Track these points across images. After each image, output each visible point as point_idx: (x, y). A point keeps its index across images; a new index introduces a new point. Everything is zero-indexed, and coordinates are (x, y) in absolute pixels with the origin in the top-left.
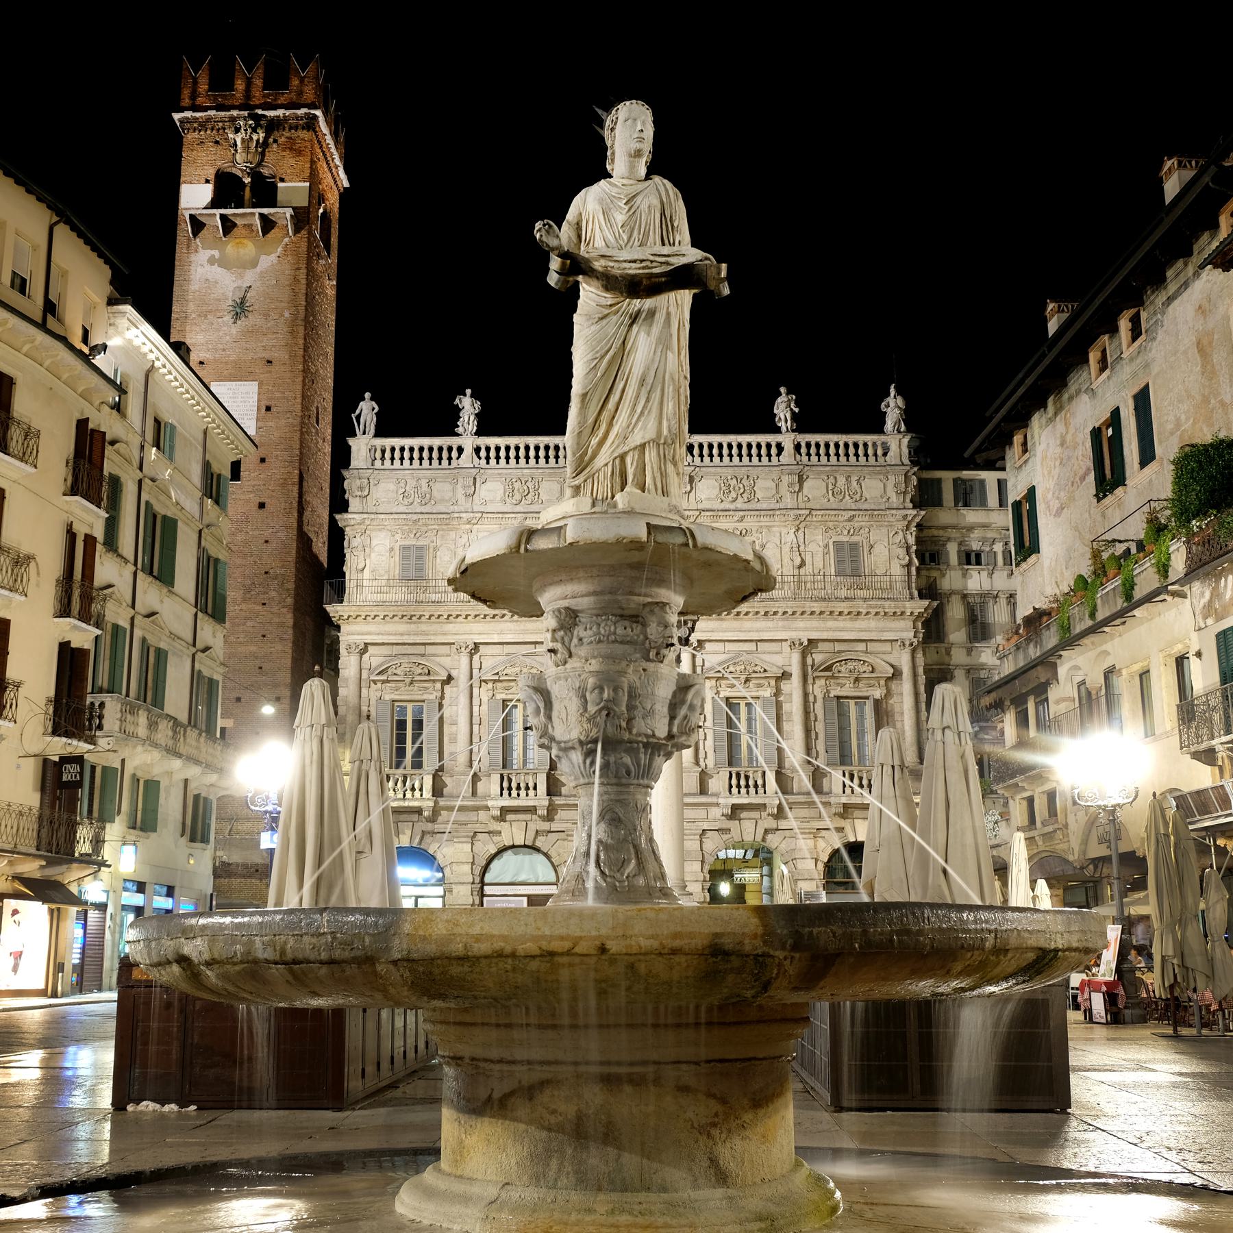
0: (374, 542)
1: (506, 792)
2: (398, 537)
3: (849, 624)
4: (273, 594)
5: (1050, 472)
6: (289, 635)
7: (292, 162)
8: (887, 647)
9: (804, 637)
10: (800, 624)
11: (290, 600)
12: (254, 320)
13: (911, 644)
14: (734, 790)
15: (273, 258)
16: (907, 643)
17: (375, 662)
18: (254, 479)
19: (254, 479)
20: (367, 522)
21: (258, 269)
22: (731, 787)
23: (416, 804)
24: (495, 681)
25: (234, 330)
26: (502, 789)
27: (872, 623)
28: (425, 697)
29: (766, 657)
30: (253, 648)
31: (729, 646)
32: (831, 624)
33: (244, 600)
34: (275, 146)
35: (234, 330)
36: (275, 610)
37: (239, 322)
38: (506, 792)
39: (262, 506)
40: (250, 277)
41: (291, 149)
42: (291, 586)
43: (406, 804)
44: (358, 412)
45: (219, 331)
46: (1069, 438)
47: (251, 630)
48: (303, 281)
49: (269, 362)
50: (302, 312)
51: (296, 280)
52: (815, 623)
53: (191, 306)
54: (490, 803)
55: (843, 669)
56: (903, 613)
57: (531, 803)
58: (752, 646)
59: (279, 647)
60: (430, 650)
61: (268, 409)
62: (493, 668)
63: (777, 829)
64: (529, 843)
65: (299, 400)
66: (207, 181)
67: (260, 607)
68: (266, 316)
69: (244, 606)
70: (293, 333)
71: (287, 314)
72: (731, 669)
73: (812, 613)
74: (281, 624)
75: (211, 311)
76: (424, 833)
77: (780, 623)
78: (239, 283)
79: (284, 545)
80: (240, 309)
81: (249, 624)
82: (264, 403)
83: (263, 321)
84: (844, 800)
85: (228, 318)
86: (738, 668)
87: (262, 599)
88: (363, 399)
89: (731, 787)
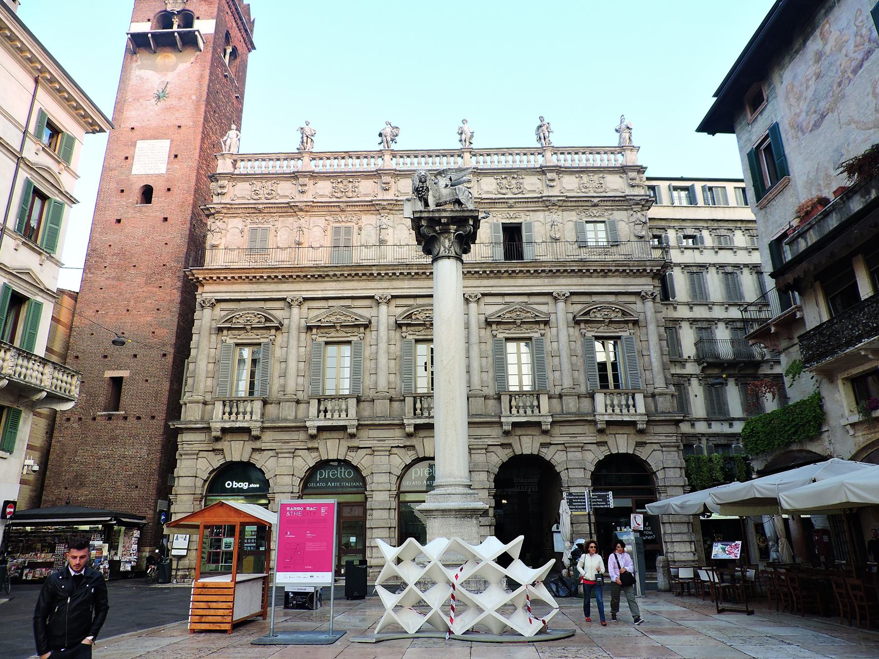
0: (230, 226)
1: (322, 414)
2: (249, 221)
3: (601, 281)
5: (798, 99)
7: (206, 8)
8: (632, 299)
9: (567, 290)
10: (562, 281)
11: (179, 284)
13: (652, 294)
14: (514, 411)
15: (188, 64)
16: (650, 293)
17: (223, 313)
18: (161, 202)
19: (161, 202)
20: (225, 211)
21: (177, 71)
22: (511, 407)
23: (245, 425)
24: (318, 327)
25: (156, 108)
26: (319, 411)
27: (620, 280)
28: (262, 340)
29: (535, 306)
30: (149, 319)
31: (508, 299)
32: (586, 280)
33: (146, 284)
39: (166, 219)
40: (170, 77)
43: (238, 425)
44: (225, 138)
46: (828, 49)
47: (149, 305)
49: (179, 127)
50: (204, 97)
51: (202, 76)
52: (575, 281)
53: (129, 94)
54: (308, 424)
55: (599, 316)
56: (645, 270)
57: (342, 423)
58: (525, 299)
60: (269, 305)
61: (176, 156)
62: (317, 316)
63: (551, 444)
64: (341, 457)
65: (198, 151)
66: (149, 20)
67: (157, 289)
68: (179, 99)
69: (145, 289)
70: (197, 108)
71: (194, 97)
72: (508, 315)
73: (573, 271)
76: (254, 450)
77: (546, 280)
78: (163, 79)
79: (179, 246)
84: (607, 418)
85: (153, 101)
86: (514, 315)
87: (158, 284)
88: (230, 129)
89: (511, 407)
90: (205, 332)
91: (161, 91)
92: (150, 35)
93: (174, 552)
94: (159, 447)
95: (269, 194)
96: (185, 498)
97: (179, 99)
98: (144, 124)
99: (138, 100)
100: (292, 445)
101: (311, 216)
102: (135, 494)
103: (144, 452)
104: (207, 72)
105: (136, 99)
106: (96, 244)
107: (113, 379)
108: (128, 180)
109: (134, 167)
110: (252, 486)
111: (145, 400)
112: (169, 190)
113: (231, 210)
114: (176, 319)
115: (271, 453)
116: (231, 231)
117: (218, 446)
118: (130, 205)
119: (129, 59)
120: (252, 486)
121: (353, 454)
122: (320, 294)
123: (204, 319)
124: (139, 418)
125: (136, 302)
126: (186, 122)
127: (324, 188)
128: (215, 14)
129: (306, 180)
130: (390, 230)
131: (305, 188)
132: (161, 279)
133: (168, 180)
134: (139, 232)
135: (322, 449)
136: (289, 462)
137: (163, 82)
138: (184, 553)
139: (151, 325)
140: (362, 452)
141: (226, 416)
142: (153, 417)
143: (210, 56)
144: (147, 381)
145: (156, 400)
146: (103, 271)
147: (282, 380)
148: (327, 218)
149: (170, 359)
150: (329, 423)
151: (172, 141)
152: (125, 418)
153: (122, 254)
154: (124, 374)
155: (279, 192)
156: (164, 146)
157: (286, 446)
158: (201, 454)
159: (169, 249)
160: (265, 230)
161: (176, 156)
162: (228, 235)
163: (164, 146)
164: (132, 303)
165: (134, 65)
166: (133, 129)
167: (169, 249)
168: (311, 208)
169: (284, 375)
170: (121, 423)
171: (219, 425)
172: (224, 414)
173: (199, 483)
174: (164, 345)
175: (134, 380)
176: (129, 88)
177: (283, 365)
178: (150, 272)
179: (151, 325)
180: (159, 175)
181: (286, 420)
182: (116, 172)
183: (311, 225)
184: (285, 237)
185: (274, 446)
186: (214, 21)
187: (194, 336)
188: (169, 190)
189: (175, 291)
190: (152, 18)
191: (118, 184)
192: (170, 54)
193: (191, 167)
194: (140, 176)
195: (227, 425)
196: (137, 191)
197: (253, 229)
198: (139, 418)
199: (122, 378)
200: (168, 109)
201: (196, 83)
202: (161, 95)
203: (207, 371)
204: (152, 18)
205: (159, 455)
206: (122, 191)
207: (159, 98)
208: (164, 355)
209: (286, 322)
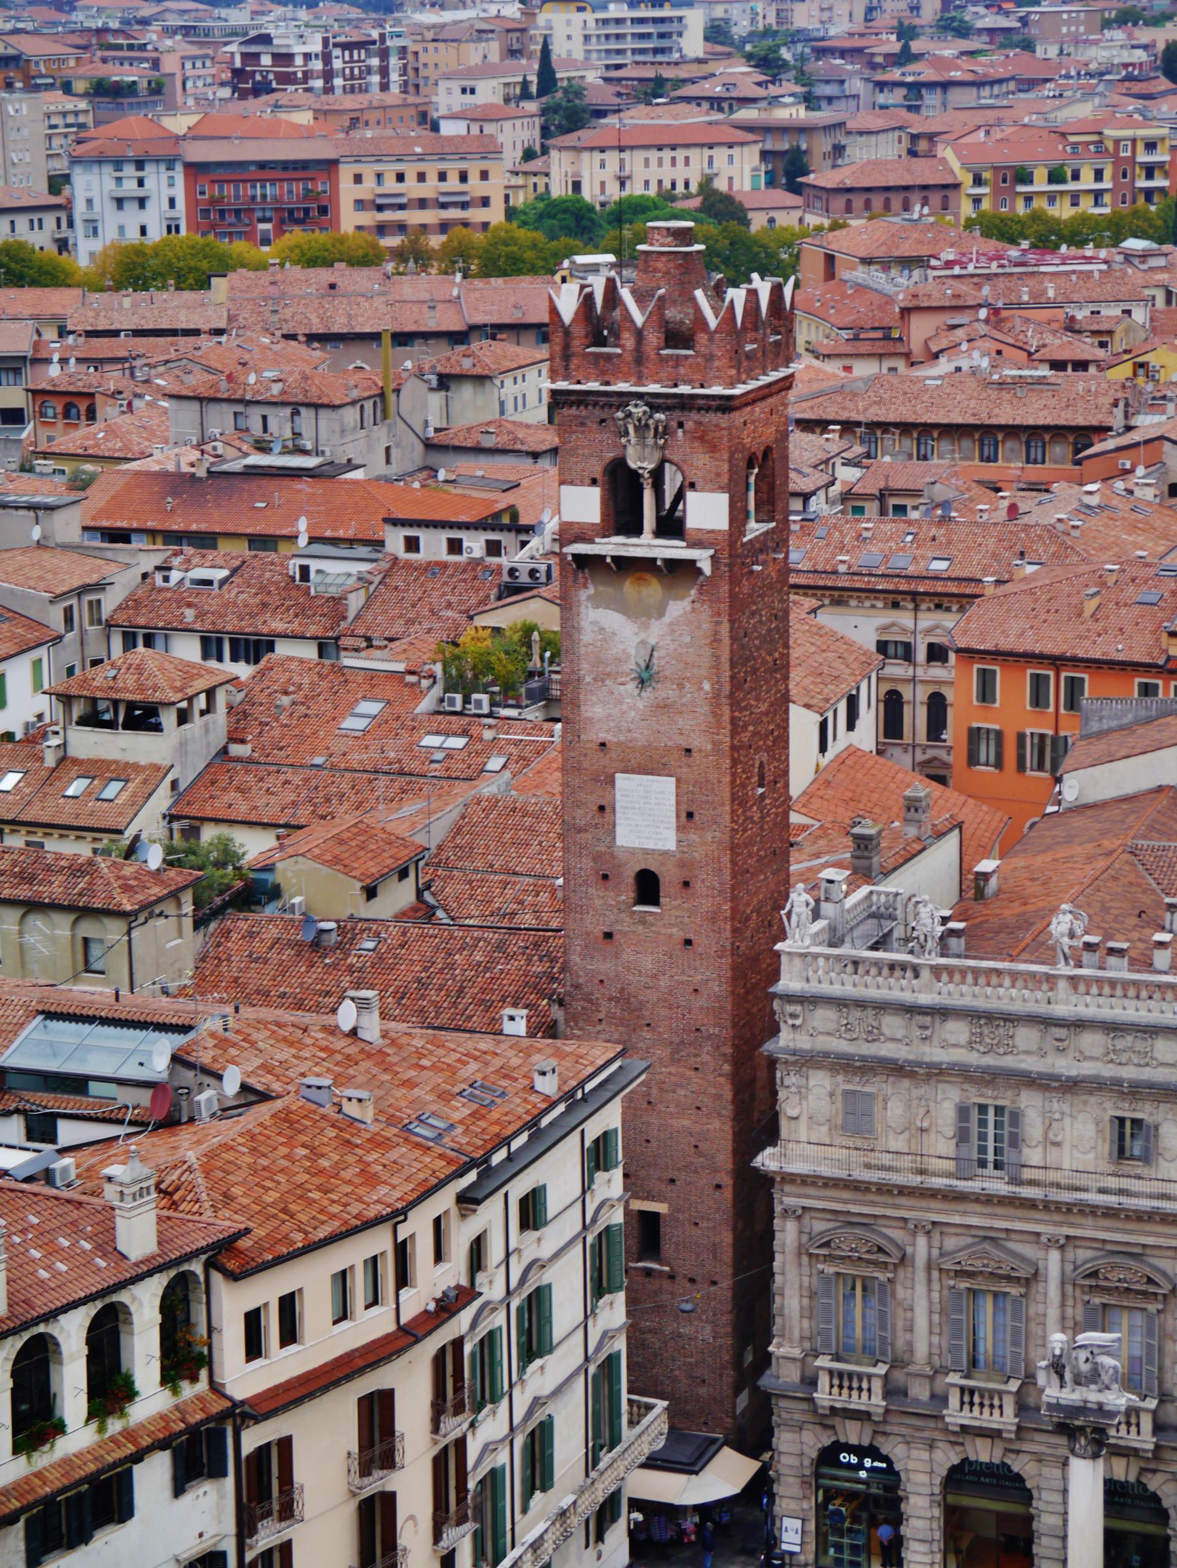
0: (812, 1083)
1: (966, 1407)
4: (706, 1058)
6: (728, 1111)
11: (727, 1068)
12: (666, 691)
18: (676, 908)
19: (676, 908)
21: (667, 619)
26: (962, 1403)
30: (686, 1122)
34: (680, 432)
35: (640, 704)
36: (711, 1077)
37: (643, 694)
38: (966, 1407)
39: (688, 942)
40: (656, 631)
41: (702, 439)
42: (729, 1050)
43: (852, 1406)
45: (621, 703)
48: (727, 641)
49: (688, 751)
50: (726, 689)
51: (715, 640)
53: (585, 665)
59: (717, 1124)
61: (690, 815)
66: (594, 482)
68: (681, 686)
69: (673, 1070)
71: (707, 686)
74: (718, 1097)
75: (609, 675)
76: (875, 1432)
78: (643, 636)
80: (645, 679)
81: (683, 1092)
82: (684, 807)
83: (677, 692)
85: (631, 687)
90: (790, 1255)
91: (643, 665)
92: (608, 560)
93: (784, 1547)
94: (729, 1329)
95: (870, 1032)
96: (791, 1480)
97: (681, 686)
98: (622, 738)
99: (603, 681)
100: (926, 1434)
101: (939, 1081)
102: (703, 1391)
103: (707, 1332)
104: (725, 628)
105: (600, 679)
106: (578, 977)
107: (642, 1213)
108: (612, 855)
109: (619, 830)
110: (876, 1464)
111: (698, 1255)
112: (686, 884)
113: (809, 1061)
114: (728, 1128)
115: (899, 1439)
116: (815, 1090)
117: (829, 1422)
118: (623, 907)
119: (571, 578)
120: (876, 1464)
121: (1013, 1456)
122: (957, 1219)
123: (787, 1235)
124: (692, 1280)
125: (661, 1090)
126: (698, 741)
127: (958, 1031)
128: (725, 480)
129: (927, 1020)
130: (1067, 1121)
131: (928, 1033)
132: (696, 1056)
133: (682, 864)
134: (648, 963)
135: (968, 1446)
136: (925, 1455)
137: (643, 642)
138: (797, 1549)
139: (691, 1134)
140: (1024, 1458)
141: (835, 1390)
142: (714, 1283)
143: (725, 588)
144: (696, 1224)
145: (715, 1257)
146: (599, 1028)
147: (908, 1336)
148: (965, 1086)
149: (728, 1194)
150: (977, 1423)
151: (678, 781)
152: (672, 1277)
153: (623, 998)
154: (661, 1208)
155: (885, 1030)
156: (663, 789)
157: (918, 1434)
158: (806, 1426)
159: (701, 1002)
160: (869, 1095)
161: (690, 815)
162: (810, 1097)
163: (663, 789)
164: (654, 1091)
165: (583, 595)
166: (603, 744)
167: (701, 1002)
168: (936, 1073)
169: (910, 1329)
170: (666, 1284)
171: (827, 1404)
172: (832, 1386)
173: (807, 1462)
174: (716, 1171)
175: (677, 1220)
176: (583, 650)
177: (909, 1314)
178: (677, 1040)
179: (691, 1134)
180: (665, 853)
181: (916, 1401)
182: (587, 837)
183: (940, 1097)
184: (899, 1111)
185: (903, 1431)
186: (726, 497)
187: (777, 1256)
188: (686, 884)
189: (722, 1080)
190: (598, 476)
191: (595, 860)
192: (648, 576)
193: (720, 843)
194: (632, 851)
195: (838, 1405)
196: (633, 874)
197: (846, 1093)
198: (692, 1280)
199: (655, 1216)
200: (663, 707)
201: (707, 652)
202: (645, 675)
203: (802, 1308)
204: (598, 475)
205: (730, 1341)
206: (605, 877)
207: (642, 682)
208: (718, 1187)
209: (909, 1250)
